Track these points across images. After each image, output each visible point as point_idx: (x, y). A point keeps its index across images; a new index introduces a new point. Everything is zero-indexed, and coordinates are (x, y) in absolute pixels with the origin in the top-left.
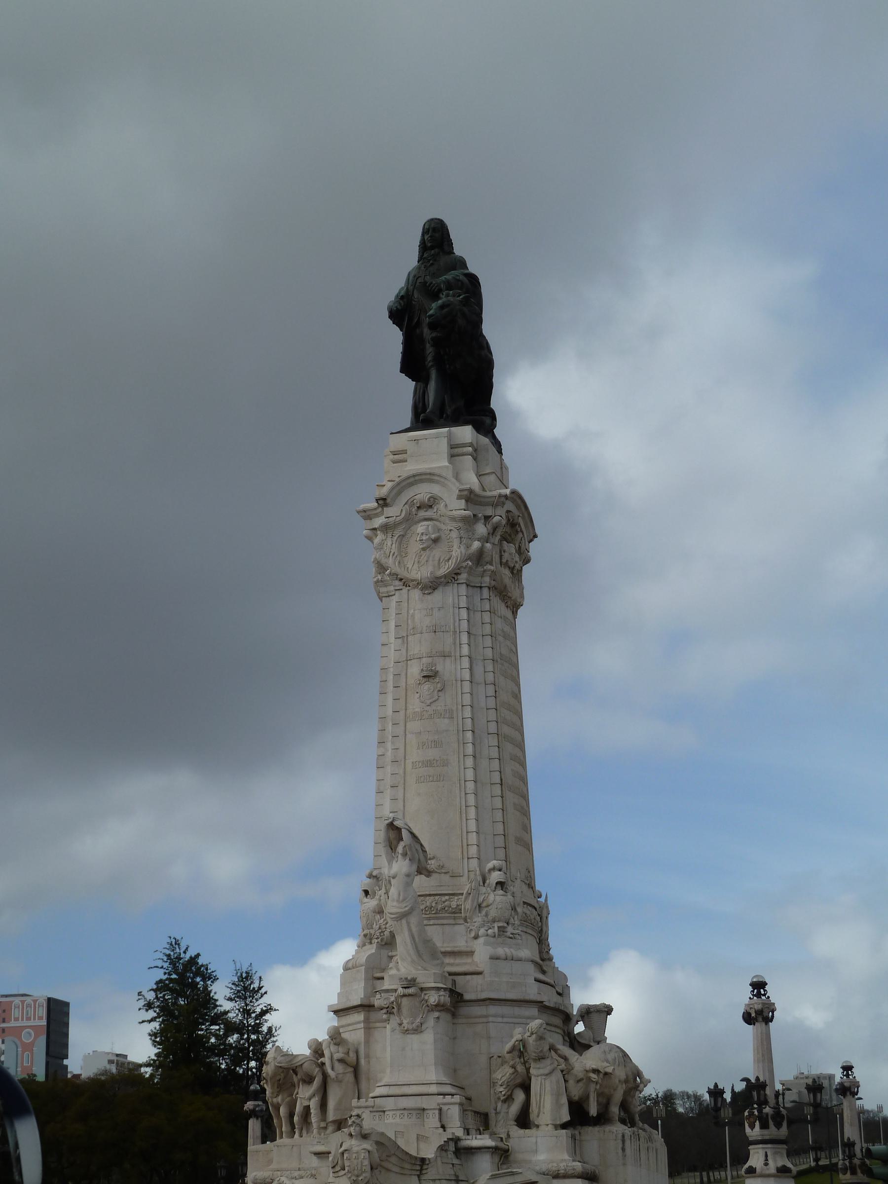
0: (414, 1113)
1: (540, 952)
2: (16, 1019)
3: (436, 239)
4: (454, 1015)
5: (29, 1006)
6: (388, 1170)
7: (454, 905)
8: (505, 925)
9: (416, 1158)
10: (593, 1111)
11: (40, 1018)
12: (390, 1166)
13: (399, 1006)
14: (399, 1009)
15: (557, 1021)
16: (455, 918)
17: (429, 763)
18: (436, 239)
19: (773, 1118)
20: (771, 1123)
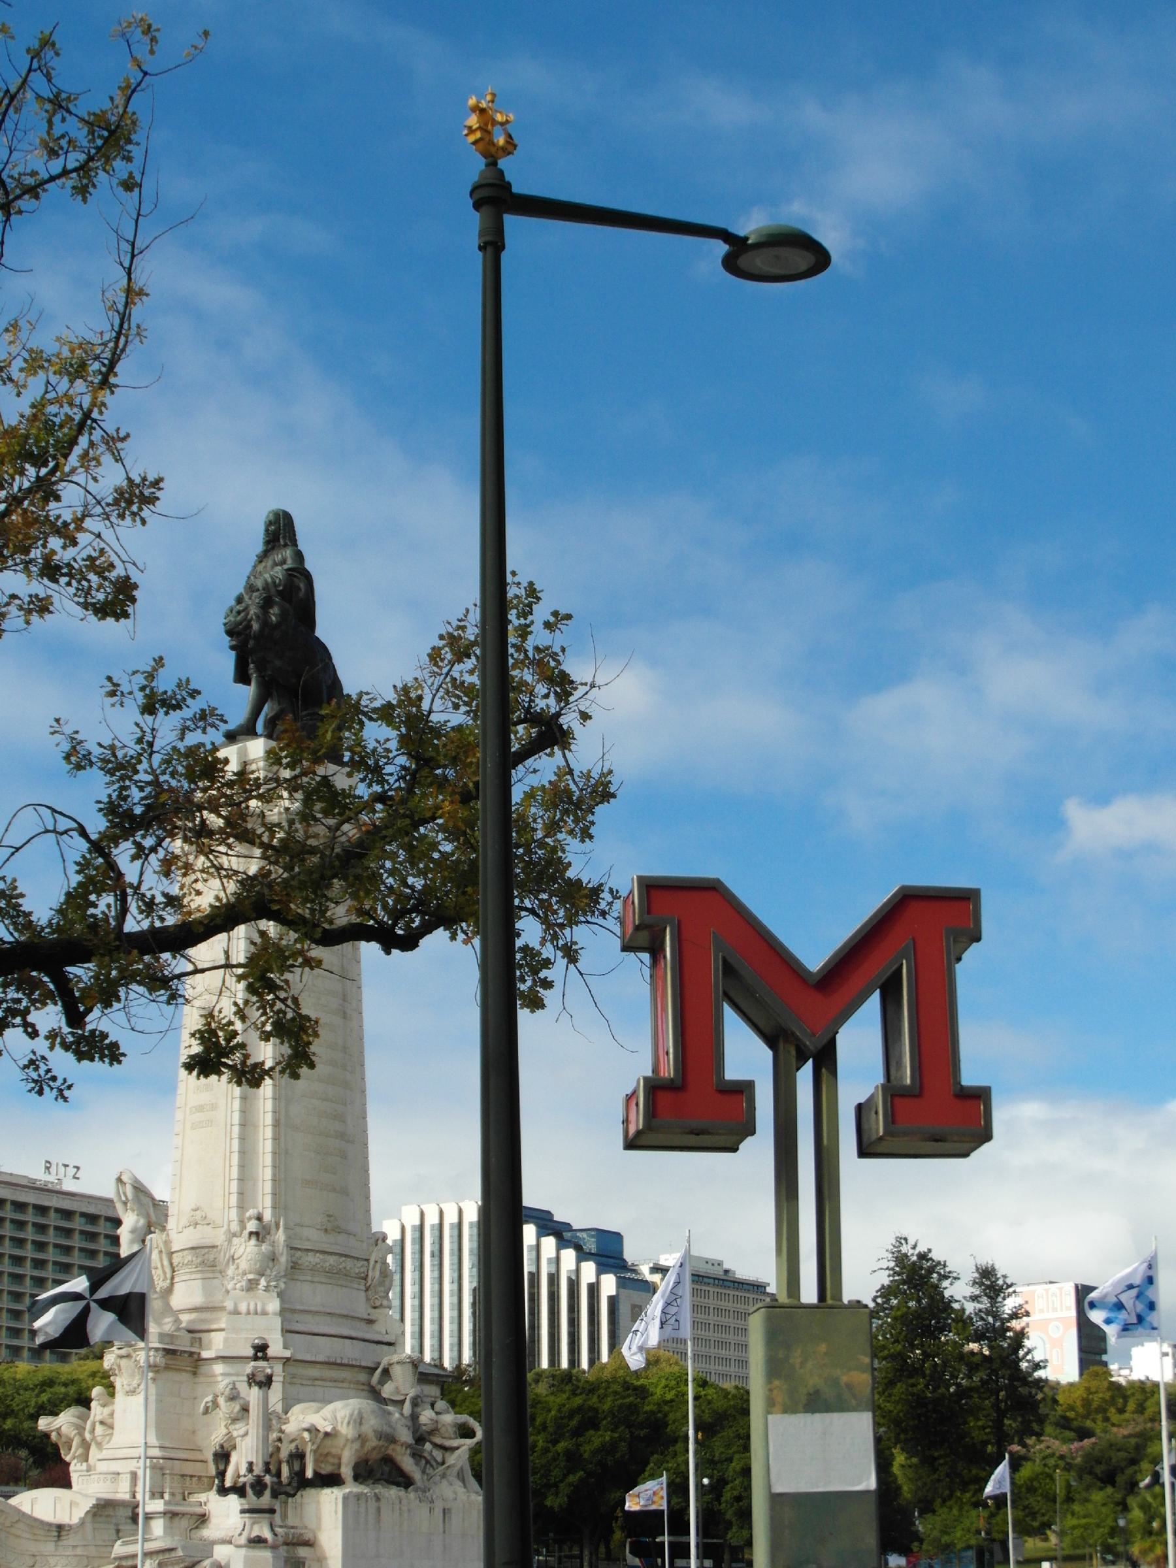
0: (109, 1477)
1: (368, 1299)
2: (1041, 1311)
3: (281, 531)
4: (195, 1373)
5: (1054, 1294)
6: (17, 1536)
7: (211, 1257)
8: (257, 1277)
9: (50, 1525)
10: (309, 1474)
11: (1068, 1308)
12: (19, 1533)
13: (119, 1366)
14: (120, 1370)
15: (362, 1377)
16: (213, 1272)
17: (200, 1108)
18: (281, 531)
19: (253, 1486)
20: (249, 1491)
